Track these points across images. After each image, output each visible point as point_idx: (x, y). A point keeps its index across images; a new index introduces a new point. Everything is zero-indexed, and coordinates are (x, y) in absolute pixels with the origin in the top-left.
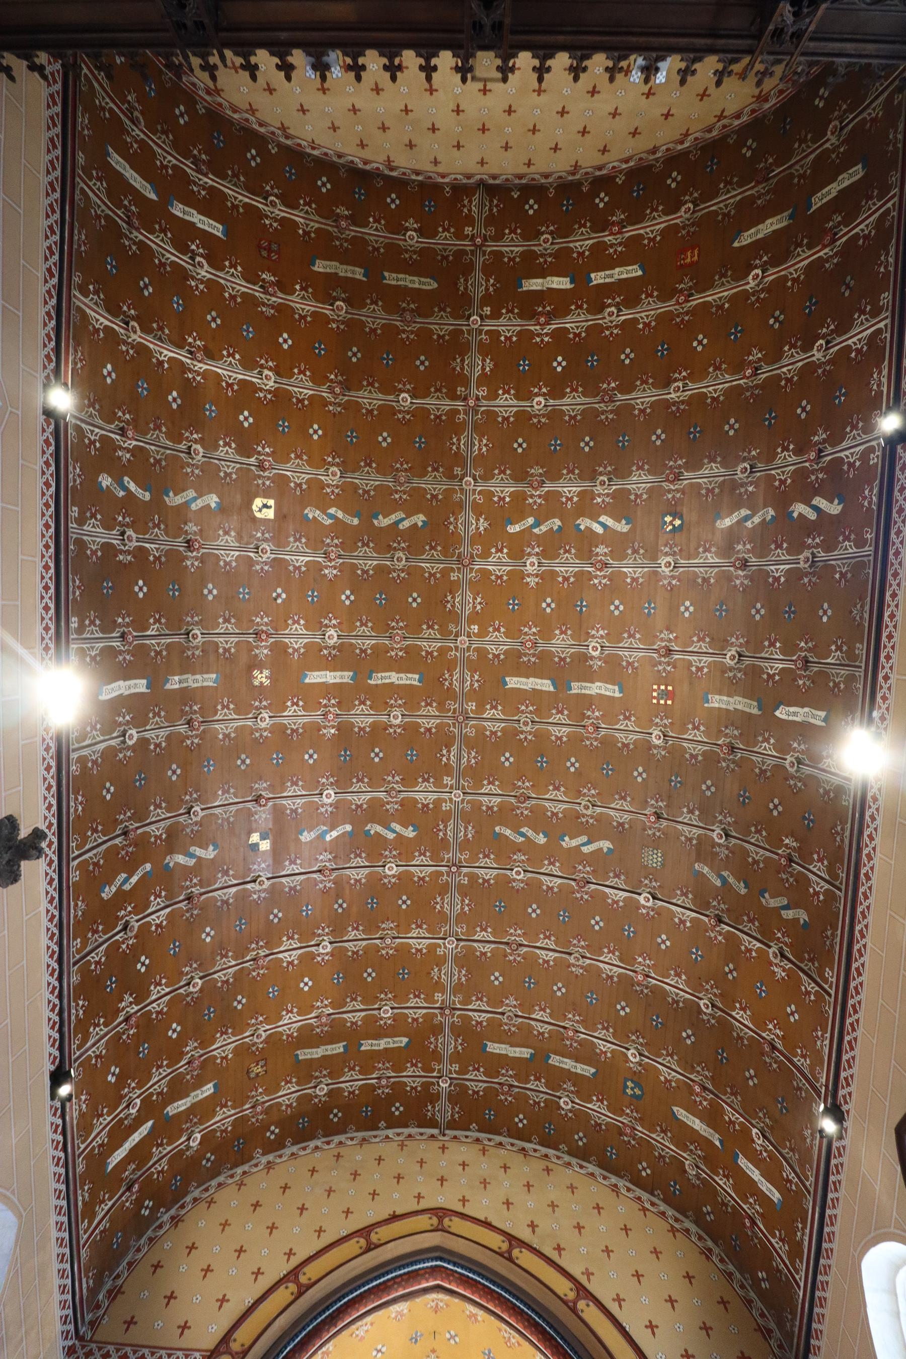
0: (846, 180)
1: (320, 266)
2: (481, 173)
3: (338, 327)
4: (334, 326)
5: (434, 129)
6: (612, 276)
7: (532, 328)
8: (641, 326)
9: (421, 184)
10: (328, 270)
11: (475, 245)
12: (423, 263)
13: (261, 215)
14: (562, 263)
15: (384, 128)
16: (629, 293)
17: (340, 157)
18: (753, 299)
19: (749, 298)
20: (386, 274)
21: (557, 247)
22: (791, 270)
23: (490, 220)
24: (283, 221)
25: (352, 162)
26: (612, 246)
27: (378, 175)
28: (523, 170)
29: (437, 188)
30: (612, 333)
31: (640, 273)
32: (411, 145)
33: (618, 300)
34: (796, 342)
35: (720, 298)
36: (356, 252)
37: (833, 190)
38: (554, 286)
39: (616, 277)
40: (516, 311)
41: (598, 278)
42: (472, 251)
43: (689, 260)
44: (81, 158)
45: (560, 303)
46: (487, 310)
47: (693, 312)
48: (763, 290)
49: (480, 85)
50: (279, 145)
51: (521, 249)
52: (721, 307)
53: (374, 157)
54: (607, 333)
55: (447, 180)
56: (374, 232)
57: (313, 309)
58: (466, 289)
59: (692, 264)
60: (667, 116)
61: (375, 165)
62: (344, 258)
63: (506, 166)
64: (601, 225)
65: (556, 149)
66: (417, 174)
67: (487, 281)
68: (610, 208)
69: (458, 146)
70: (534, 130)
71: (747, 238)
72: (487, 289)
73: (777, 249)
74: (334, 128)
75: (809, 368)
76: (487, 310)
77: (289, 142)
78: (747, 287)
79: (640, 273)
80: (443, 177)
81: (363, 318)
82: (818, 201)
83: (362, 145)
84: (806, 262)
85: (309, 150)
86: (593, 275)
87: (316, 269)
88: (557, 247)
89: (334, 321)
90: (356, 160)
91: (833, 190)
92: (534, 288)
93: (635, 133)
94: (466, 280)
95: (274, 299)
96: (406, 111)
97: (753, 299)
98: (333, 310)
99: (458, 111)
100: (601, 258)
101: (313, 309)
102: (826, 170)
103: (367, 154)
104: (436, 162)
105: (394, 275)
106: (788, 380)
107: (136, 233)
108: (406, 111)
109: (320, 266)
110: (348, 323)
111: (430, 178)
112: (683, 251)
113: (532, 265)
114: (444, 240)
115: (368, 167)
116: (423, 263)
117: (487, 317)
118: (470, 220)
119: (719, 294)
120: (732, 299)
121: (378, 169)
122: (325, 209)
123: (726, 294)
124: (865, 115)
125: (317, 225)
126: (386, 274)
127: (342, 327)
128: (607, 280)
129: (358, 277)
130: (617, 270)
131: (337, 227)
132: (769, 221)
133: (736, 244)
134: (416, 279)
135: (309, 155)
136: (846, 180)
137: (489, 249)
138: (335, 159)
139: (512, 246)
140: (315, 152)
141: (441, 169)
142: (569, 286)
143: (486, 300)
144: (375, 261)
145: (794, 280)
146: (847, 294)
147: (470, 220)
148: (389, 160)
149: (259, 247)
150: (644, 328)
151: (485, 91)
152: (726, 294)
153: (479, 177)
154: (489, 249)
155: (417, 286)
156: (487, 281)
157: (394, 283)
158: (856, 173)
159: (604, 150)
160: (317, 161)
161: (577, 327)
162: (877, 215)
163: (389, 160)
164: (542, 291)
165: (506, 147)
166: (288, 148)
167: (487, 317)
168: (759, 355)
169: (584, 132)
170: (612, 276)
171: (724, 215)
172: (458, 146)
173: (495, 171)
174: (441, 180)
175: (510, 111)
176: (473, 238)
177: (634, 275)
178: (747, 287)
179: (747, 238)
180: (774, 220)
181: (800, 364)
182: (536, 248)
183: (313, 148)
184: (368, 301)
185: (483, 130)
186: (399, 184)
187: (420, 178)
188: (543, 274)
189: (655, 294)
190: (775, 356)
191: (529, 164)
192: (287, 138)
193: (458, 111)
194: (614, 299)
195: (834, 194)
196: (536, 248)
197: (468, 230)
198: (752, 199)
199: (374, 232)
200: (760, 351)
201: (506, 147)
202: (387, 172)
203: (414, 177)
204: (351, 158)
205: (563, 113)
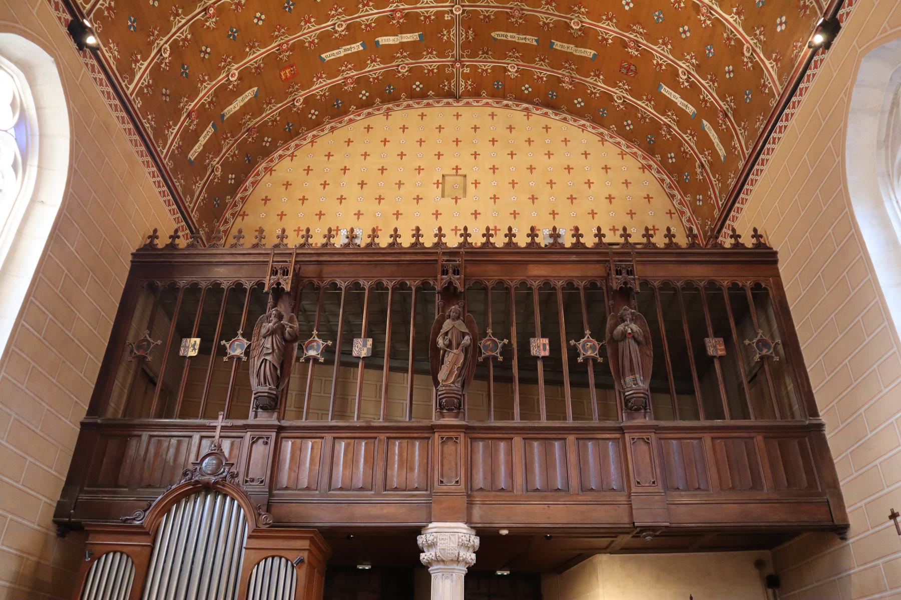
0: (198, 148)
1: (590, 53)
2: (458, 107)
3: (580, 8)
4: (583, 10)
5: (493, 141)
6: (345, 50)
7: (406, 6)
8: (312, 20)
9: (504, 98)
10: (583, 50)
11: (461, 62)
12: (504, 49)
13: (630, 92)
14: (388, 54)
15: (529, 141)
16: (328, 41)
17: (565, 119)
18: (229, 60)
19: (233, 59)
20: (535, 43)
21: (394, 64)
22: (209, 87)
23: (449, 78)
24: (615, 85)
25: (556, 114)
26: (350, 69)
27: (537, 104)
28: (426, 111)
29: (493, 95)
30: (336, 10)
31: (323, 56)
32: (511, 128)
33: (337, 35)
34: (184, 43)
35: (254, 53)
36: (560, 60)
37: (203, 140)
38: (392, 38)
39: (341, 50)
40: (422, 18)
41: (357, 47)
42: (463, 56)
43: (287, 71)
44: (741, 165)
45: (384, 26)
46: (447, 17)
47: (273, 39)
48: (224, 67)
49: (460, 172)
50: (609, 129)
51: (422, 60)
52: (251, 48)
53: (539, 118)
54: (340, 10)
55: (485, 101)
56: (542, 71)
57: (600, 24)
58: (467, 32)
59: (284, 69)
60: (329, 155)
61: (538, 112)
62: (568, 57)
63: (440, 113)
64: (361, 82)
65: (404, 128)
66: (507, 105)
67: (449, 38)
68: (356, 91)
69: (475, 128)
70: (421, 142)
71: (249, 94)
72: (449, 32)
73: (224, 95)
74: (566, 141)
75: (165, 31)
76: (447, 17)
77: (601, 130)
78: (236, 66)
79: (323, 56)
80: (487, 103)
81: (556, 13)
82: (210, 130)
83: (547, 128)
84: (201, 95)
85: (588, 124)
86: (361, 48)
87: (593, 52)
88: (394, 64)
89: (583, 14)
90: (553, 116)
91: (203, 140)
92: (409, 35)
93: (349, 142)
94: (467, 38)
95: (631, 36)
96: (512, 154)
97: (229, 60)
98: (582, 22)
99: (475, 155)
100: (358, 60)
101: (600, 24)
102: (213, 147)
103: (545, 121)
104: (493, 115)
105: (528, 42)
106: (177, 15)
107: (725, 107)
108: (512, 154)
109: (590, 53)
110: (570, 10)
111: (497, 103)
112: (293, 76)
113: (413, 50)
114: (486, 64)
115: (545, 110)
116: (504, 49)
117: (447, 12)
118: (466, 77)
119: (255, 57)
120: (244, 55)
121: (537, 109)
122: (580, 89)
123: (251, 57)
124: (202, 182)
125: (588, 79)
126: (535, 43)
127: (576, 8)
128: (349, 47)
129: (559, 43)
130: (342, 55)
131: (572, 77)
132: (237, 108)
133: (255, 89)
134: (509, 39)
135: (588, 121)
136: (198, 148)
137: (449, 59)
138: (569, 117)
139: (430, 62)
140: (583, 122)
141: (489, 110)
142: (380, 39)
143: (449, 25)
144: (545, 51)
145: (204, 81)
146: (164, 90)
147: (466, 77)
148: (528, 116)
149: (636, 73)
150: (309, 19)
151: (457, 169)
152: (251, 57)
153: (460, 104)
154: (449, 59)
155: (509, 34)
156: (449, 38)
157: (528, 37)
158: (193, 155)
159: (368, 128)
160: (582, 116)
161: (367, 11)
162: (169, 142)
163: (528, 116)
164: (401, 33)
165: (440, 128)
166: (603, 126)
167: (447, 12)
168: (208, 24)
169: (385, 141)
170: (345, 50)
171: (270, 103)
172: (475, 128)
173: (447, 109)
174: (490, 101)
175: (439, 155)
176: (463, 66)
177: (328, 54)
178: (236, 66)
179: (249, 94)
180: (234, 111)
181: (174, 30)
182: (411, 61)
183: (584, 125)
184: (551, 25)
185: (457, 141)
186: (521, 98)
187: (505, 102)
188: (403, 45)
189: (307, 44)
190: (196, 28)
191: (422, 115)
192: (602, 134)
193: (475, 155)
194: (340, 35)
195: (201, 138)
196: (411, 61)
197: (467, 70)
198: (254, 116)
199: (542, 71)
200: (208, 27)
201: (440, 128)
202: (530, 106)
203: (510, 103)
204: (557, 118)
205: (402, 155)
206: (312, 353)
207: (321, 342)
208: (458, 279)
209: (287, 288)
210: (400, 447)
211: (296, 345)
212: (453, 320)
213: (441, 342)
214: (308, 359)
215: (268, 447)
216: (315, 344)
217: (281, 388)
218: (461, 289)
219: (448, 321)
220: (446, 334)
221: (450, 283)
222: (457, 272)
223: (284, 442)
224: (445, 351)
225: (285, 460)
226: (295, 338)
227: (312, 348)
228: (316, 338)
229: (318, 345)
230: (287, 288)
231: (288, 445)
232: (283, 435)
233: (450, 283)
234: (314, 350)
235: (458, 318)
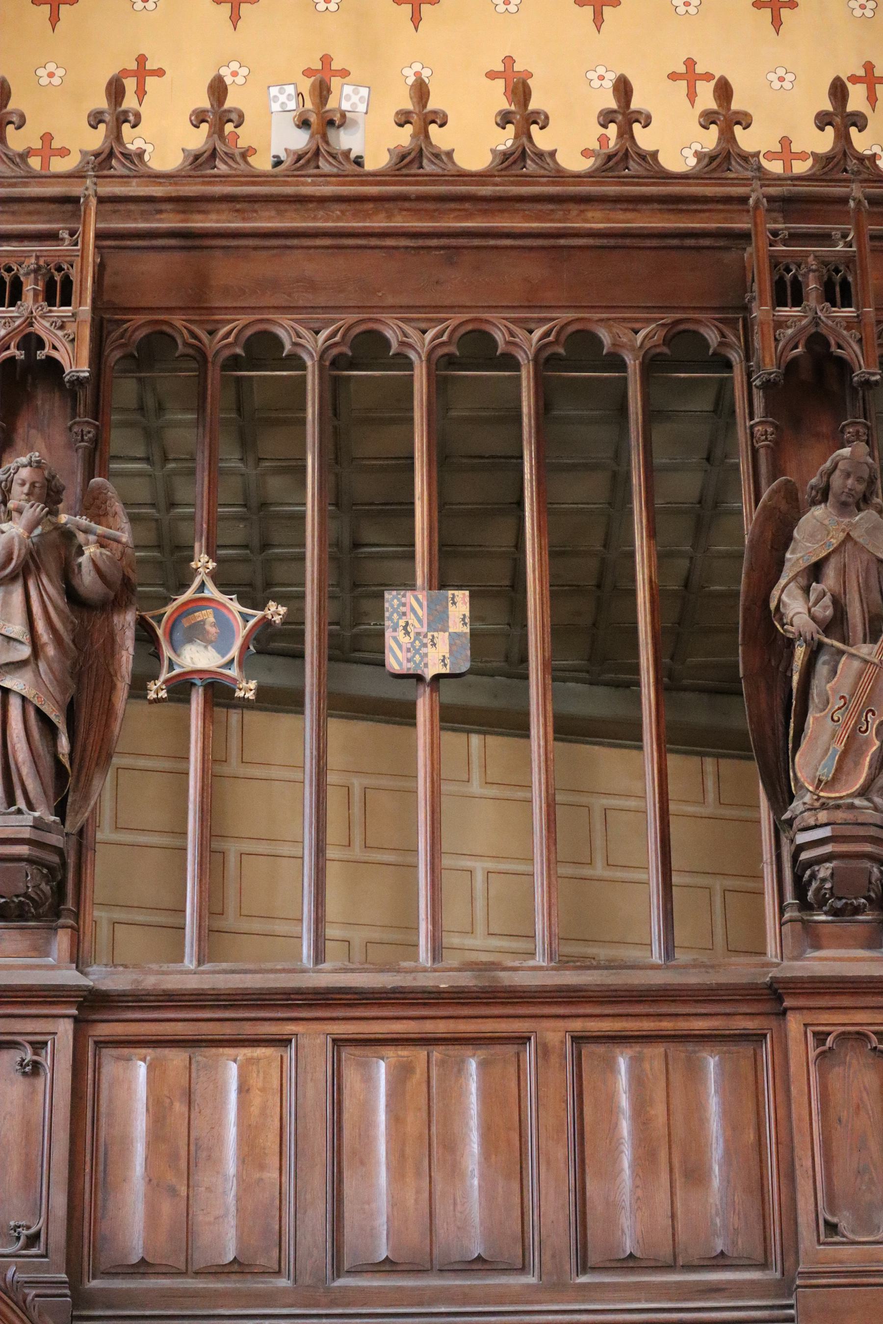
206: (198, 658)
207: (235, 606)
208: (849, 325)
209: (76, 362)
210: (638, 1082)
211: (126, 622)
212: (844, 507)
213: (796, 609)
214: (181, 689)
215: (40, 1083)
216: (207, 616)
217: (73, 824)
218: (865, 368)
219: (818, 511)
220: (816, 571)
221: (817, 342)
222: (838, 291)
223: (111, 1067)
224: (815, 651)
225: (126, 1142)
226: (121, 592)
227: (196, 633)
228: (212, 591)
229: (223, 623)
230: (76, 362)
231: (134, 1082)
232: (103, 1030)
233: (817, 342)
234: (207, 642)
235: (863, 501)
